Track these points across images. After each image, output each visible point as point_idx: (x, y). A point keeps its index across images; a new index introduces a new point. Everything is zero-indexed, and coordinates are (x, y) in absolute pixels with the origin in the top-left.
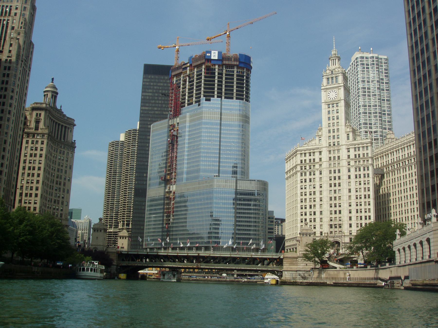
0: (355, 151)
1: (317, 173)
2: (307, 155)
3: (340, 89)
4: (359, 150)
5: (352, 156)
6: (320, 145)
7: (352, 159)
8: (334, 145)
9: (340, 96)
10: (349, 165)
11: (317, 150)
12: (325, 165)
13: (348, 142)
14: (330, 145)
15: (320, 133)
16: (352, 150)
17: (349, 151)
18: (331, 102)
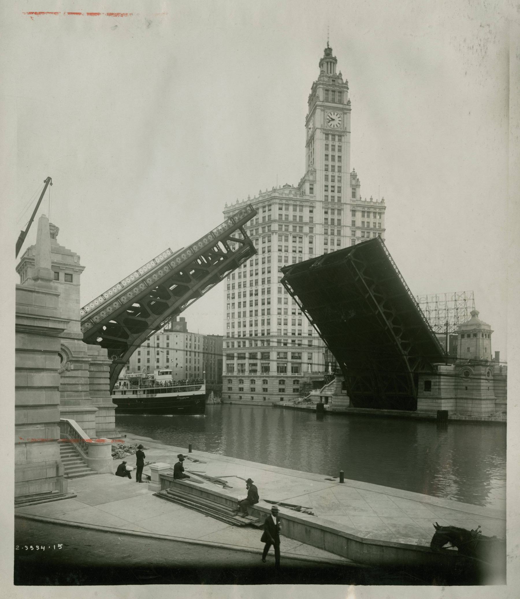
0: (363, 216)
1: (306, 240)
2: (291, 208)
3: (346, 113)
4: (368, 216)
5: (359, 224)
6: (312, 197)
7: (358, 228)
8: (333, 200)
9: (345, 126)
10: (354, 235)
11: (307, 204)
12: (319, 229)
13: (353, 201)
14: (326, 200)
15: (311, 178)
16: (359, 215)
17: (354, 215)
18: (331, 130)
